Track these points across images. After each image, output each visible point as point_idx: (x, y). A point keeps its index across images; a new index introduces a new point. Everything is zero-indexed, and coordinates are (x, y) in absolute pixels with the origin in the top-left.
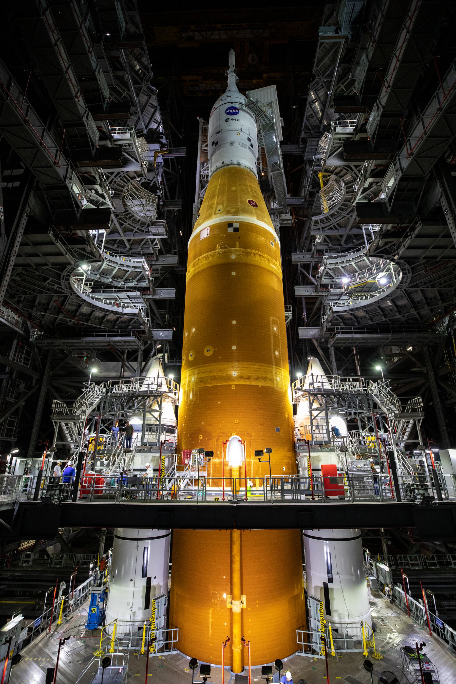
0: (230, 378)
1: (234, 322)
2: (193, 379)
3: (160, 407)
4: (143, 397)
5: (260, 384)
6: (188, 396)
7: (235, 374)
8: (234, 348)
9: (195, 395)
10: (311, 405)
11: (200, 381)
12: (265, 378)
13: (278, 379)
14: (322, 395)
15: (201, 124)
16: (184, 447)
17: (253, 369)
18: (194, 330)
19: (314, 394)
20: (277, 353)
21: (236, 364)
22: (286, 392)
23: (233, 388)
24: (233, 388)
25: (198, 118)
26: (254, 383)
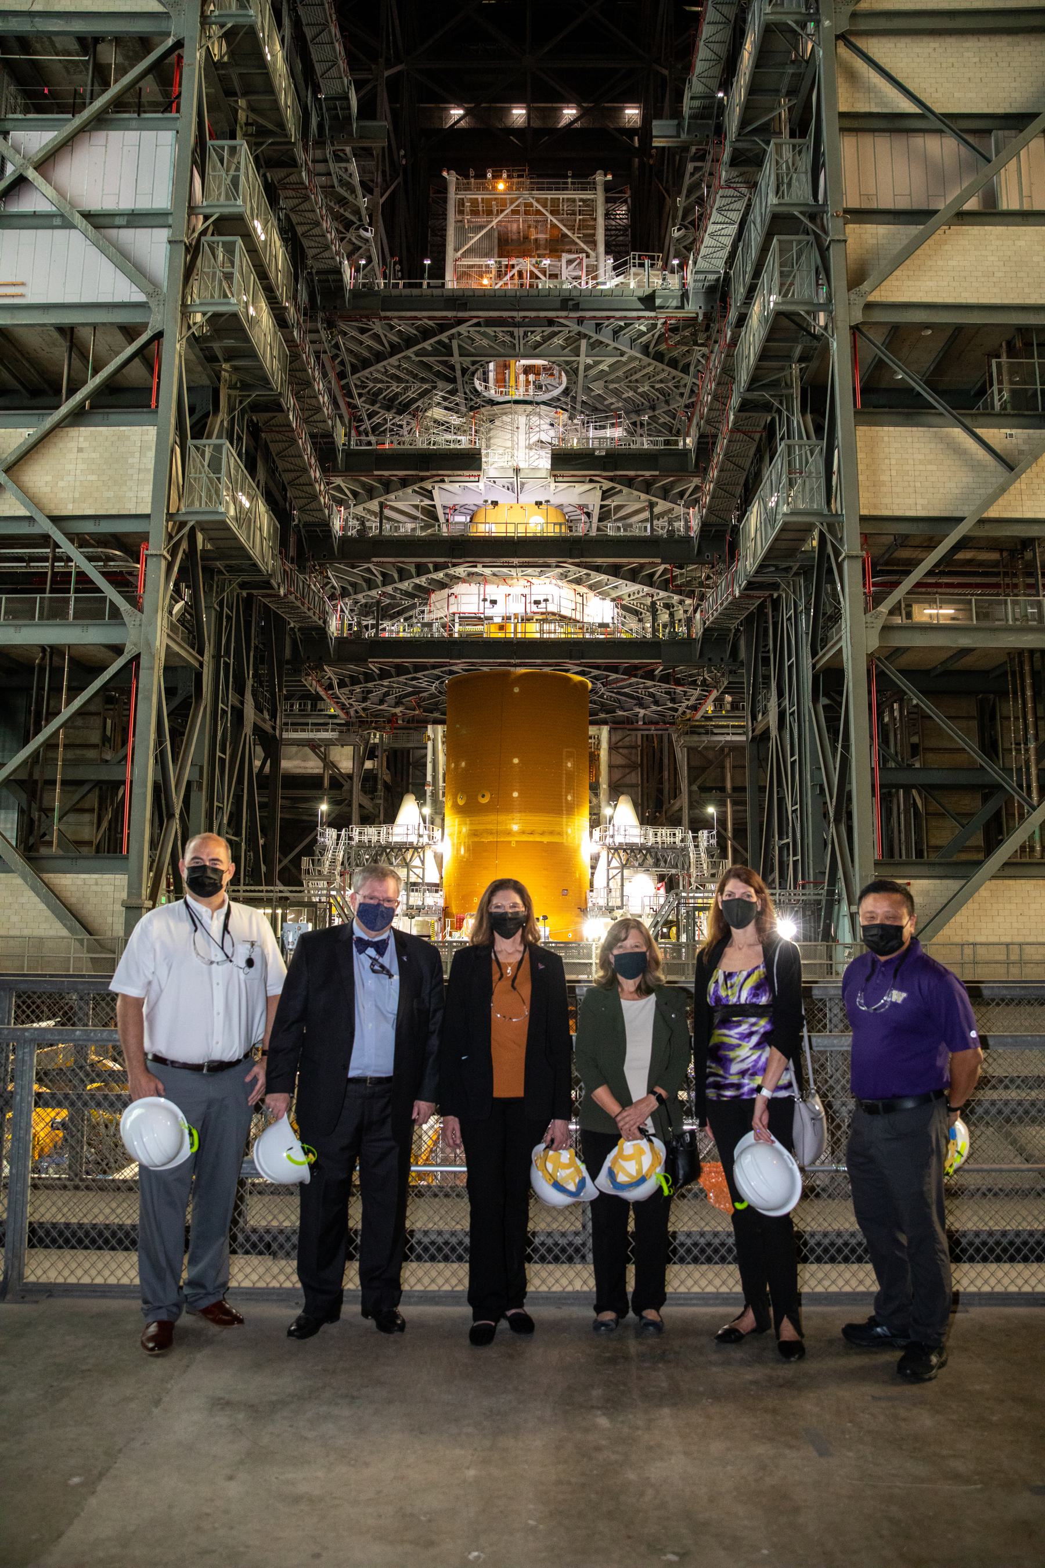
0: (509, 833)
1: (516, 761)
2: (464, 830)
3: (423, 862)
4: (400, 849)
5: (545, 839)
6: (458, 850)
7: (515, 828)
8: (515, 794)
9: (468, 850)
10: (609, 863)
11: (474, 833)
12: (551, 833)
13: (569, 831)
14: (625, 850)
15: (452, 189)
16: (454, 910)
17: (539, 821)
18: (463, 764)
19: (616, 849)
20: (569, 798)
21: (517, 816)
22: (579, 846)
23: (513, 845)
24: (513, 845)
25: (445, 174)
26: (538, 839)
